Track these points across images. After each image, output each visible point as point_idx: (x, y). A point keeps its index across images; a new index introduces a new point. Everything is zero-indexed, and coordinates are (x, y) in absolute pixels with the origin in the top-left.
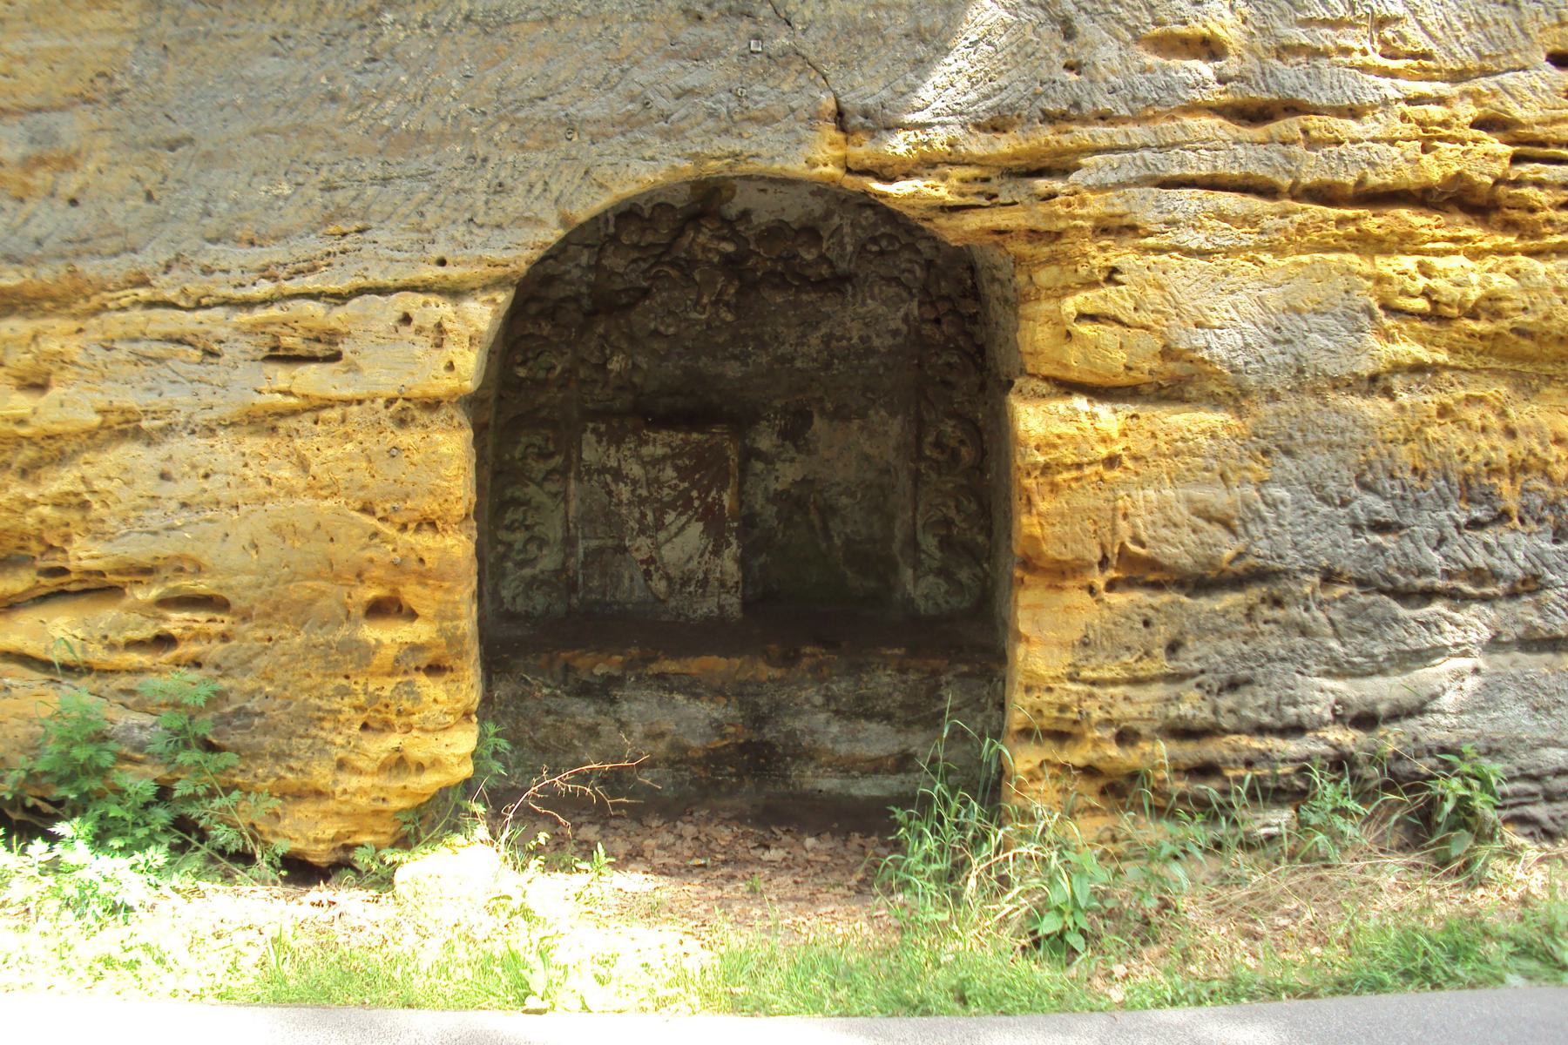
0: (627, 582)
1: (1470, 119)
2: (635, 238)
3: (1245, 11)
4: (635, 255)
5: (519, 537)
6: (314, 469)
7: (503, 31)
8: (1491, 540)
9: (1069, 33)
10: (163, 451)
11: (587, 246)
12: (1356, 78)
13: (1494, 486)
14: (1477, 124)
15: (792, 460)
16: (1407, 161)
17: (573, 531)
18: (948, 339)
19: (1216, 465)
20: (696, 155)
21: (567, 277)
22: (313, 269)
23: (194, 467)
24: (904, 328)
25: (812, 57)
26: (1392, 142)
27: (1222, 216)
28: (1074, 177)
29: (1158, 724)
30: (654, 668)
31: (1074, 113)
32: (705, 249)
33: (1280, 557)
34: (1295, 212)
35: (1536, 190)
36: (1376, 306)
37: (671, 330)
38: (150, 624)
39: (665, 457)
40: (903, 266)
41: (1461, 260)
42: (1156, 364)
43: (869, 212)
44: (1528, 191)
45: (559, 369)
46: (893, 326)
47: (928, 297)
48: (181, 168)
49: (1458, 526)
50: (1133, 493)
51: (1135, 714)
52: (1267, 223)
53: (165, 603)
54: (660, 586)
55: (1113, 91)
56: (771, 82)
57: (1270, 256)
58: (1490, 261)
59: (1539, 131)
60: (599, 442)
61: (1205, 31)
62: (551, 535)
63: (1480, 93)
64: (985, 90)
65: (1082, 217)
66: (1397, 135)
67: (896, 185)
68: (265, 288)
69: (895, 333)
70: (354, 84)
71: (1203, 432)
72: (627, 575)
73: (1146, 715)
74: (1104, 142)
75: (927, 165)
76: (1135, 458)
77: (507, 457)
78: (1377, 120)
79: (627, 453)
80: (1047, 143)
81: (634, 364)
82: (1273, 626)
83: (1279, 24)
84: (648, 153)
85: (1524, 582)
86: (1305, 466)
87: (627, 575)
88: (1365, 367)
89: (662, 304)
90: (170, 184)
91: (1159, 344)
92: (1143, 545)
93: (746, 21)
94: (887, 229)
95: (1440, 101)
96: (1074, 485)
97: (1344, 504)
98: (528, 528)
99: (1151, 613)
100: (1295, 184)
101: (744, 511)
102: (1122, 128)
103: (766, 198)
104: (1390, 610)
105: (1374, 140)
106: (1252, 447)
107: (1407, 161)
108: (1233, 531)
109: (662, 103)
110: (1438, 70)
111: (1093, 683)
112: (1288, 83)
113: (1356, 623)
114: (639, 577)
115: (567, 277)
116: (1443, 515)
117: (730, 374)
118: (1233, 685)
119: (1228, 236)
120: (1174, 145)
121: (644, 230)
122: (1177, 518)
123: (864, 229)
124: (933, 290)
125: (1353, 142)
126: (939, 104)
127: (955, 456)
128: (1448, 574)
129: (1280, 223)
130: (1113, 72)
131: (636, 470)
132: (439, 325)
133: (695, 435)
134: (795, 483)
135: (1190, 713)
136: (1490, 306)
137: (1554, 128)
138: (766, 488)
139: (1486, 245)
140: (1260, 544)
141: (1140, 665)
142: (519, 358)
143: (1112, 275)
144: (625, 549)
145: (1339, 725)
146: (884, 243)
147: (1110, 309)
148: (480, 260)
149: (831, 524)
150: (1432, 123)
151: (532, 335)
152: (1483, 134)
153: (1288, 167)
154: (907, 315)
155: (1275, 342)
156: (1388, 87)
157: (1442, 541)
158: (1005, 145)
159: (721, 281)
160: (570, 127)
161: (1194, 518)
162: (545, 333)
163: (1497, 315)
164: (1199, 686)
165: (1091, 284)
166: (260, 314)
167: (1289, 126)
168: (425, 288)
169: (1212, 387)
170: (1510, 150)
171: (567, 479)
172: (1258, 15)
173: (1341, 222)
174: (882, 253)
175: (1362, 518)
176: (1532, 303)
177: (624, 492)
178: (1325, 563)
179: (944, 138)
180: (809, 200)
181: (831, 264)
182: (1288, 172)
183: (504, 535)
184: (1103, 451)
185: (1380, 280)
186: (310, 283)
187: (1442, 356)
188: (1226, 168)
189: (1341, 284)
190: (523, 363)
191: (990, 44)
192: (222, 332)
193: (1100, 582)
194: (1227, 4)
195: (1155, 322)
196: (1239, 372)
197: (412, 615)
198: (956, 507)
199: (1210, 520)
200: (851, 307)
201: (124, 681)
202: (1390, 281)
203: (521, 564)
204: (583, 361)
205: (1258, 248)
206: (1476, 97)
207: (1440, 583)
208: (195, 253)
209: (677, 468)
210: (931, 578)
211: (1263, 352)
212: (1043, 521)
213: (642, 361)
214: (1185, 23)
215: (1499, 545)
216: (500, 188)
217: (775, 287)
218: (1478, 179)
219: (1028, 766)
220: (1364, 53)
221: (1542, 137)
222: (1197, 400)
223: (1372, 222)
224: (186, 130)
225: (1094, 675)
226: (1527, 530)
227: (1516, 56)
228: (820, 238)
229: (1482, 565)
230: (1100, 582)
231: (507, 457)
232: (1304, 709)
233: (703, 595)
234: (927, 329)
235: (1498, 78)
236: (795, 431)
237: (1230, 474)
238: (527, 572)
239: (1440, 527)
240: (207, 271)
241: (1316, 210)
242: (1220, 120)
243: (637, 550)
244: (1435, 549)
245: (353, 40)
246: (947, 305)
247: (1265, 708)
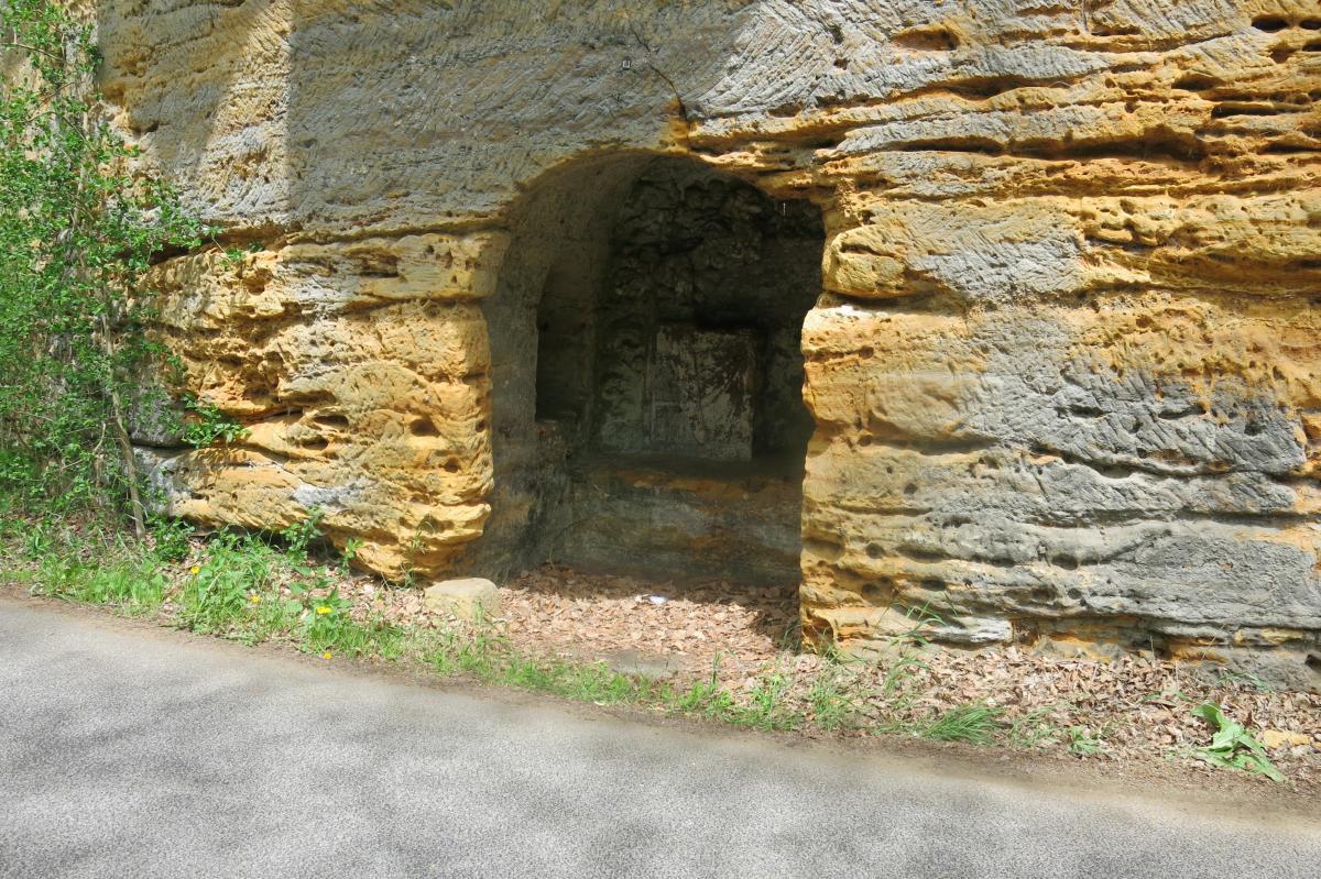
1: (1173, 80)
2: (698, 204)
3: (975, 8)
4: (698, 215)
5: (614, 398)
6: (385, 341)
7: (477, 64)
8: (1184, 429)
9: (839, 39)
10: (312, 329)
11: (662, 209)
12: (1066, 54)
13: (1187, 384)
14: (1179, 84)
16: (1110, 119)
19: (944, 357)
20: (592, 141)
22: (382, 219)
23: (327, 338)
25: (662, 70)
26: (1097, 104)
27: (951, 170)
28: (841, 146)
29: (896, 545)
30: (671, 486)
31: (840, 98)
32: (740, 211)
33: (992, 429)
34: (1012, 164)
35: (1236, 137)
36: (1081, 237)
38: (312, 431)
39: (708, 349)
41: (1166, 200)
42: (901, 282)
44: (1229, 139)
48: (312, 158)
49: (1151, 414)
50: (880, 376)
51: (879, 535)
52: (988, 174)
53: (319, 419)
54: (700, 435)
55: (869, 79)
56: (637, 89)
57: (991, 199)
58: (1194, 199)
59: (1239, 86)
61: (942, 27)
63: (1183, 58)
64: (778, 86)
65: (846, 175)
66: (1102, 98)
67: (722, 157)
68: (356, 230)
70: (397, 102)
71: (934, 332)
73: (887, 537)
74: (862, 118)
75: (740, 141)
76: (883, 350)
78: (1084, 87)
80: (822, 121)
82: (988, 480)
83: (1002, 15)
84: (563, 141)
85: (1218, 464)
86: (1017, 361)
88: (1069, 285)
90: (307, 168)
91: (901, 267)
92: (885, 413)
93: (620, 47)
95: (1146, 66)
96: (837, 368)
97: (1050, 391)
98: (621, 392)
99: (892, 463)
100: (1012, 142)
102: (876, 107)
104: (1090, 477)
105: (1081, 104)
106: (973, 345)
107: (1110, 119)
108: (956, 407)
109: (571, 108)
110: (1146, 42)
111: (851, 509)
112: (1007, 63)
113: (1059, 485)
114: (688, 427)
116: (1138, 405)
118: (957, 522)
119: (954, 185)
120: (916, 117)
121: (703, 198)
122: (912, 396)
125: (1062, 106)
126: (746, 98)
128: (1142, 453)
129: (999, 173)
130: (869, 65)
131: (688, 358)
132: (449, 254)
133: (727, 336)
135: (921, 539)
136: (1188, 234)
137: (1255, 83)
139: (1192, 185)
140: (976, 418)
141: (885, 500)
142: (618, 283)
143: (867, 216)
144: (680, 410)
145: (1044, 562)
147: (865, 242)
148: (470, 213)
150: (1136, 86)
152: (1185, 93)
153: (1006, 129)
155: (993, 266)
156: (1096, 60)
157: (1137, 427)
158: (788, 124)
160: (518, 125)
161: (925, 396)
163: (1194, 243)
164: (929, 519)
165: (854, 224)
166: (355, 246)
167: (1009, 97)
168: (435, 230)
169: (945, 299)
170: (1211, 104)
172: (985, 10)
173: (1050, 171)
175: (1065, 403)
176: (1227, 233)
177: (681, 371)
178: (1031, 435)
179: (750, 122)
182: (1005, 133)
184: (858, 345)
185: (1085, 216)
186: (378, 227)
187: (1145, 277)
188: (953, 131)
189: (1049, 219)
190: (620, 286)
191: (782, 51)
192: (336, 257)
193: (855, 439)
194: (961, 3)
195: (898, 251)
196: (963, 288)
197: (436, 433)
199: (939, 398)
201: (304, 465)
202: (1093, 216)
204: (661, 285)
205: (981, 193)
206: (1181, 62)
207: (1136, 460)
208: (321, 210)
211: (981, 273)
212: (823, 393)
214: (927, 22)
215: (1191, 432)
216: (480, 168)
218: (1178, 130)
219: (810, 564)
220: (1076, 32)
221: (1244, 91)
222: (938, 310)
223: (1078, 170)
224: (311, 135)
225: (850, 504)
226: (1217, 421)
227: (1222, 24)
229: (1174, 447)
230: (855, 439)
231: (609, 346)
232: (1012, 546)
235: (1203, 44)
237: (955, 365)
238: (619, 420)
239: (1136, 414)
240: (328, 220)
241: (1030, 163)
242: (953, 96)
244: (1131, 432)
245: (395, 74)
247: (981, 541)
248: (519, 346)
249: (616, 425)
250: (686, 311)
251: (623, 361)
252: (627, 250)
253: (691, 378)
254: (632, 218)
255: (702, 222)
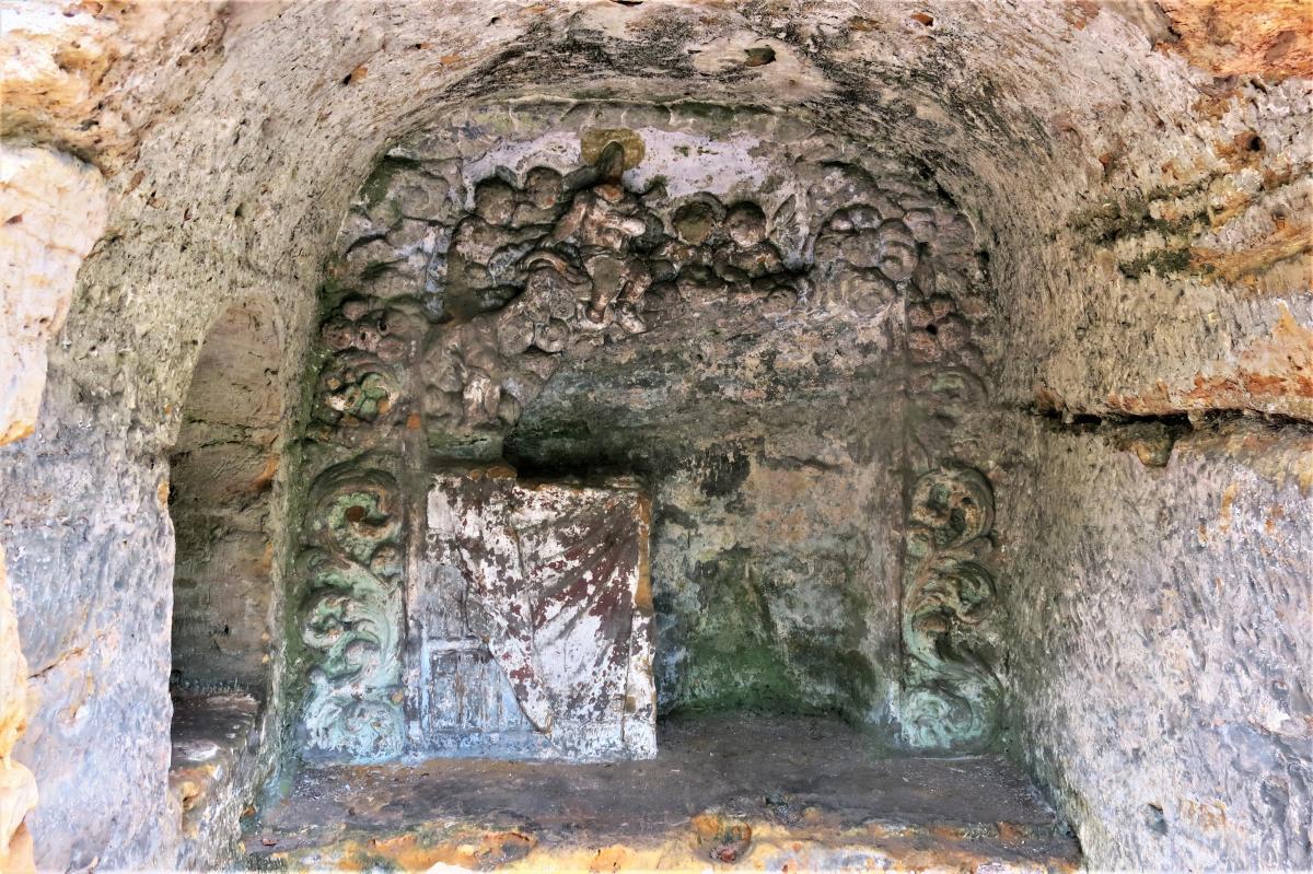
0: (492, 702)
2: (504, 216)
5: (334, 641)
11: (432, 223)
15: (721, 522)
17: (414, 631)
18: (947, 356)
21: (403, 267)
24: (882, 342)
32: (602, 230)
37: (556, 346)
39: (545, 524)
40: (884, 251)
43: (836, 174)
45: (393, 398)
46: (862, 339)
47: (921, 297)
54: (538, 710)
60: (452, 503)
62: (383, 638)
69: (867, 349)
72: (491, 691)
77: (317, 525)
79: (493, 519)
81: (503, 393)
87: (491, 691)
89: (543, 309)
94: (862, 199)
98: (349, 626)
101: (656, 590)
103: (691, 162)
114: (509, 696)
115: (403, 267)
117: (636, 406)
121: (516, 205)
123: (828, 198)
124: (925, 285)
127: (956, 523)
131: (502, 543)
133: (589, 492)
134: (724, 553)
138: (685, 560)
142: (334, 384)
144: (490, 656)
146: (858, 218)
149: (773, 608)
151: (352, 351)
154: (887, 322)
159: (624, 275)
162: (372, 348)
171: (405, 556)
174: (853, 232)
177: (488, 574)
180: (747, 162)
181: (777, 253)
183: (309, 637)
190: (341, 390)
198: (959, 593)
200: (805, 313)
203: (337, 679)
204: (431, 388)
209: (564, 540)
210: (925, 696)
213: (514, 387)
217: (701, 284)
228: (762, 216)
231: (317, 525)
233: (600, 720)
234: (918, 341)
236: (725, 479)
238: (347, 690)
243: (507, 656)
246: (946, 308)
248: (119, 585)
249: (340, 701)
250: (489, 441)
251: (353, 557)
252: (354, 311)
253: (513, 587)
254: (364, 241)
255: (517, 254)
